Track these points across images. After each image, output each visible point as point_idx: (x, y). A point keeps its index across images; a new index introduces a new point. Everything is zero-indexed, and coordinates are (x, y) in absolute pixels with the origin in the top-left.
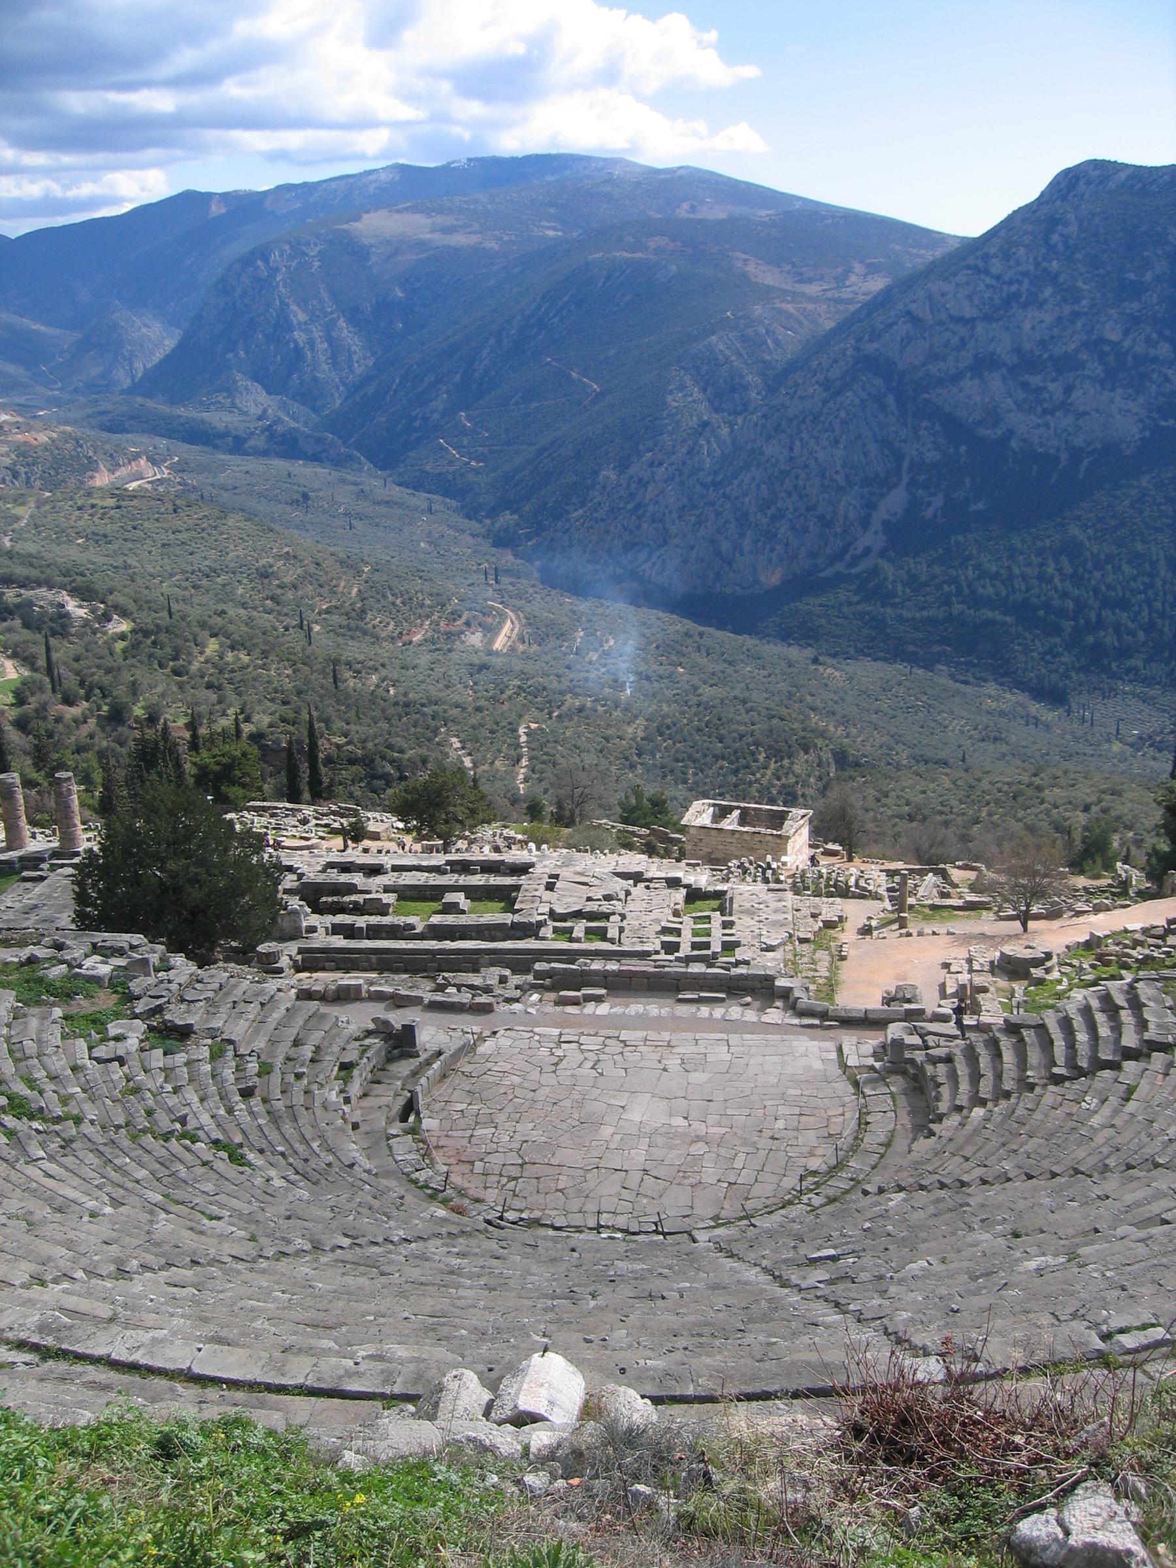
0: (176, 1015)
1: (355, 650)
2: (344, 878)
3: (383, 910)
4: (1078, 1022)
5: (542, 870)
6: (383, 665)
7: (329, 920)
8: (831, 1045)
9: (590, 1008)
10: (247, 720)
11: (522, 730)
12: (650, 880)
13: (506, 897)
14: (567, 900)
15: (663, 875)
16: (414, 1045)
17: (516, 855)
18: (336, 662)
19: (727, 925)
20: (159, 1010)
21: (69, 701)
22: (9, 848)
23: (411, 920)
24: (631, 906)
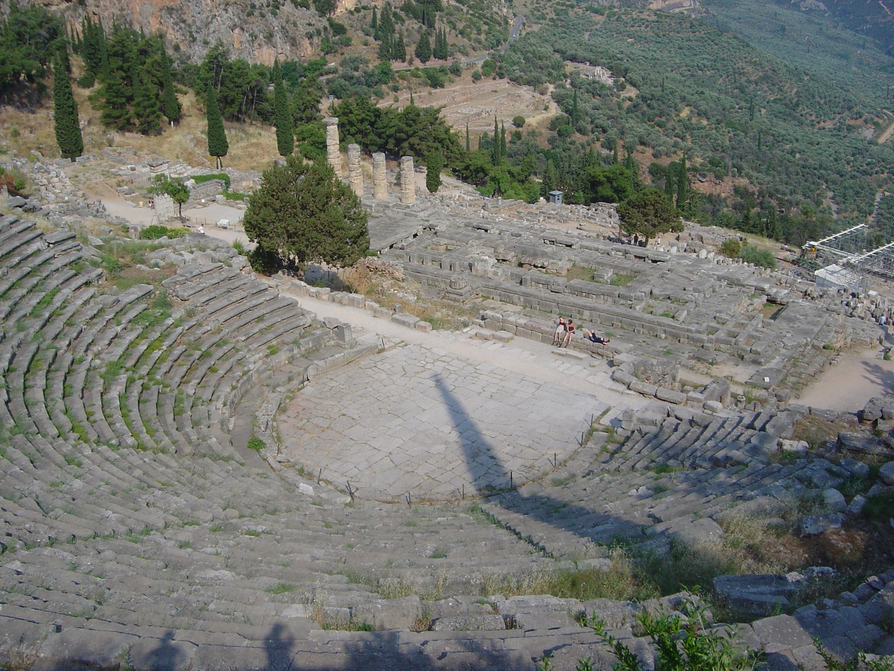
1: (781, 127)
6: (797, 140)
10: (689, 159)
12: (744, 286)
15: (755, 284)
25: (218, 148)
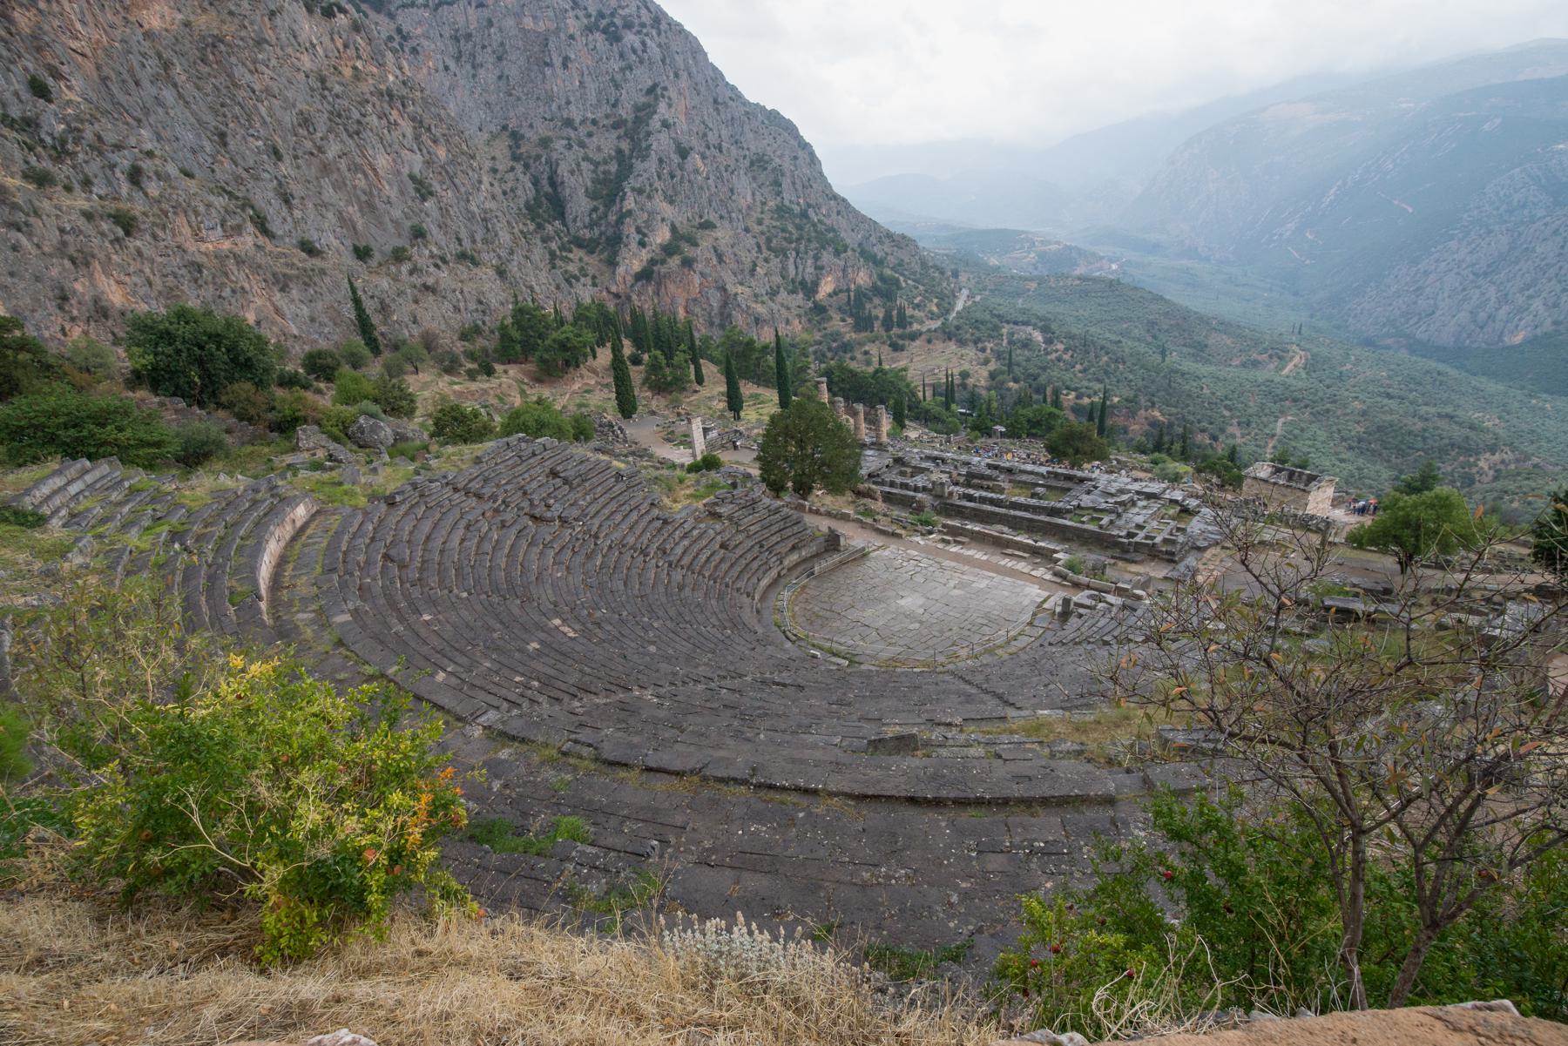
1: (1188, 365)
2: (988, 472)
3: (1001, 491)
7: (961, 490)
11: (1281, 420)
18: (1176, 372)
21: (1016, 380)
25: (734, 403)
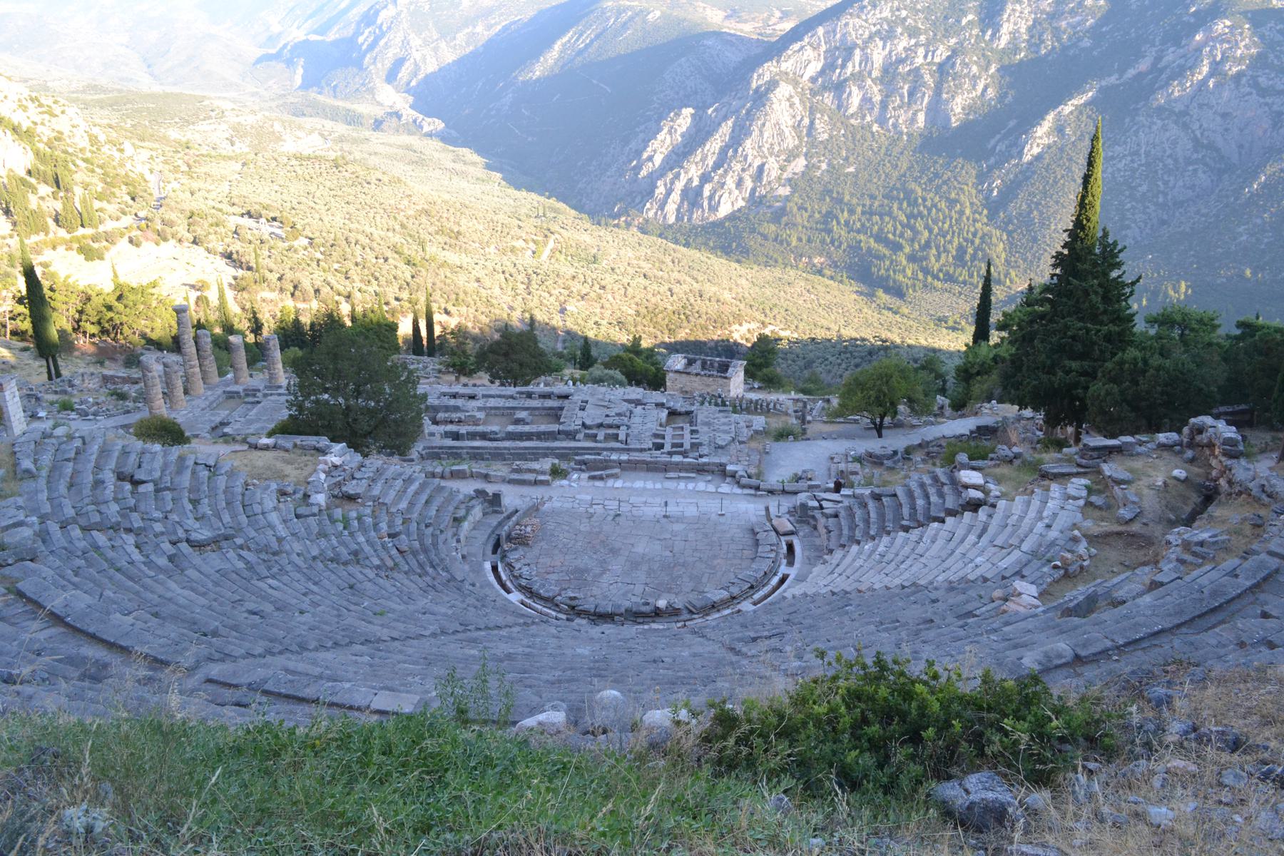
0: (351, 488)
1: (453, 257)
2: (452, 402)
4: (917, 492)
5: (577, 398)
7: (442, 428)
8: (762, 507)
9: (610, 482)
13: (555, 415)
14: (593, 415)
16: (500, 505)
17: (560, 388)
19: (693, 432)
20: (339, 484)
22: (236, 383)
23: (495, 428)
24: (633, 420)
